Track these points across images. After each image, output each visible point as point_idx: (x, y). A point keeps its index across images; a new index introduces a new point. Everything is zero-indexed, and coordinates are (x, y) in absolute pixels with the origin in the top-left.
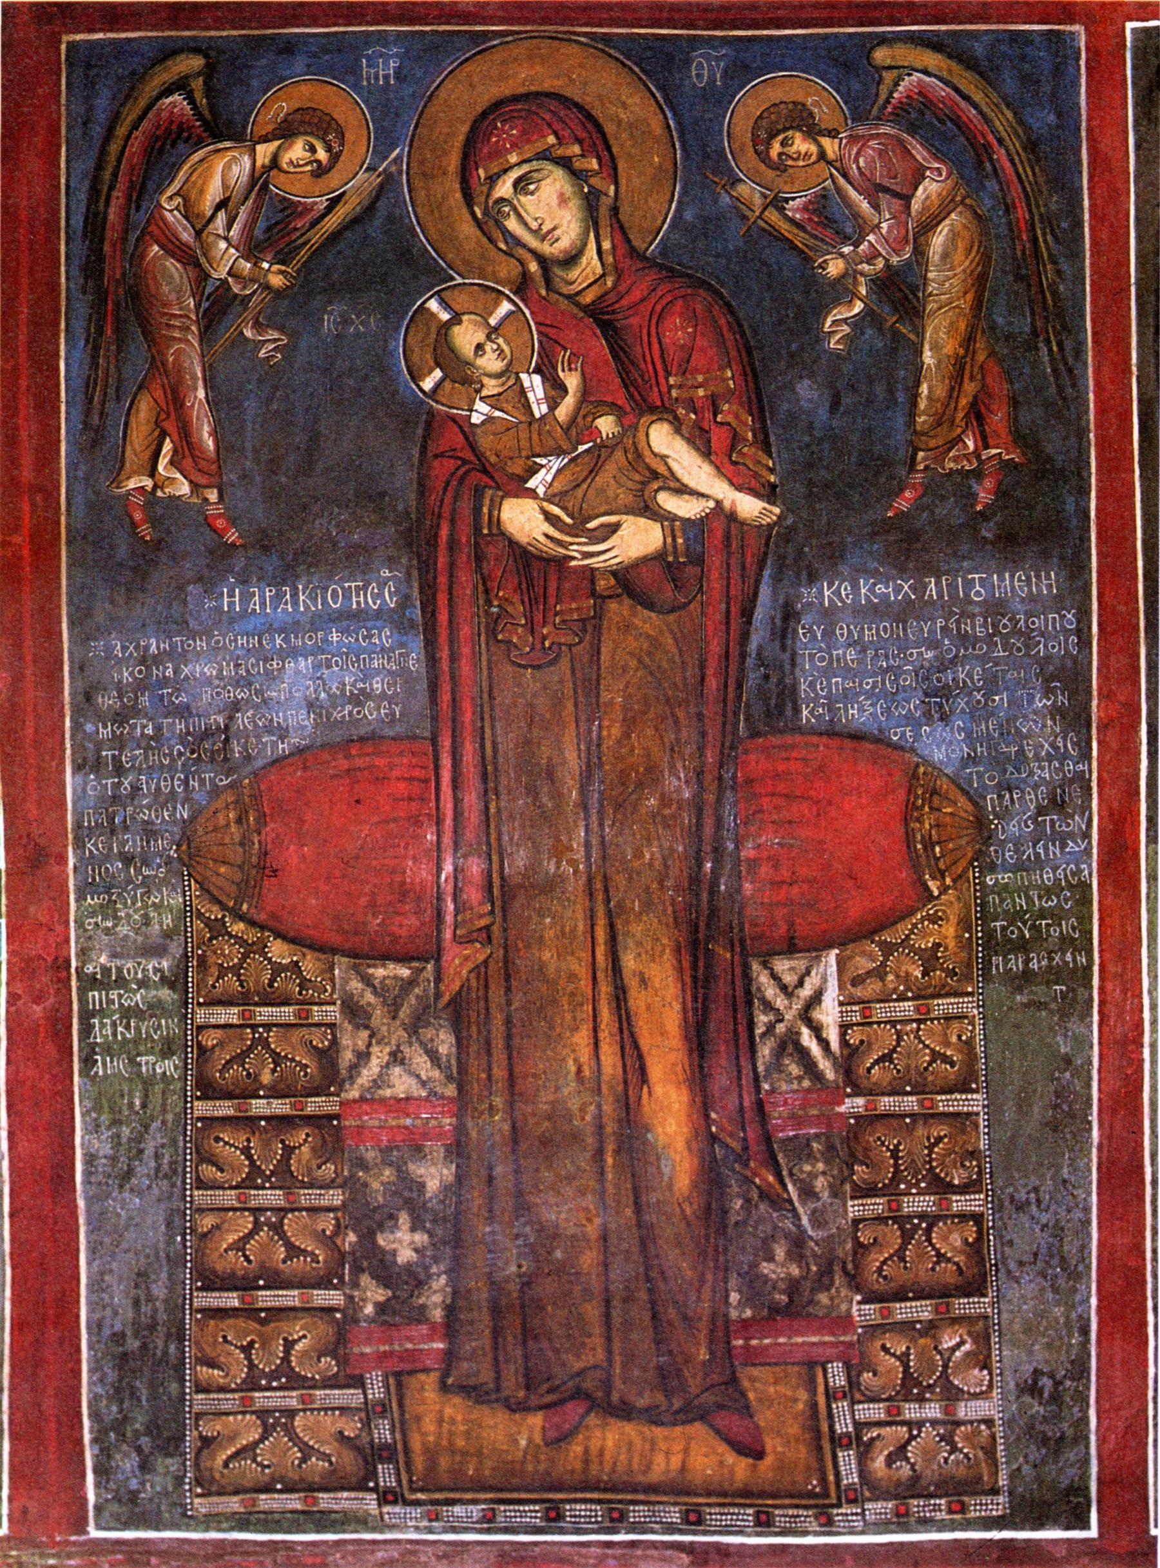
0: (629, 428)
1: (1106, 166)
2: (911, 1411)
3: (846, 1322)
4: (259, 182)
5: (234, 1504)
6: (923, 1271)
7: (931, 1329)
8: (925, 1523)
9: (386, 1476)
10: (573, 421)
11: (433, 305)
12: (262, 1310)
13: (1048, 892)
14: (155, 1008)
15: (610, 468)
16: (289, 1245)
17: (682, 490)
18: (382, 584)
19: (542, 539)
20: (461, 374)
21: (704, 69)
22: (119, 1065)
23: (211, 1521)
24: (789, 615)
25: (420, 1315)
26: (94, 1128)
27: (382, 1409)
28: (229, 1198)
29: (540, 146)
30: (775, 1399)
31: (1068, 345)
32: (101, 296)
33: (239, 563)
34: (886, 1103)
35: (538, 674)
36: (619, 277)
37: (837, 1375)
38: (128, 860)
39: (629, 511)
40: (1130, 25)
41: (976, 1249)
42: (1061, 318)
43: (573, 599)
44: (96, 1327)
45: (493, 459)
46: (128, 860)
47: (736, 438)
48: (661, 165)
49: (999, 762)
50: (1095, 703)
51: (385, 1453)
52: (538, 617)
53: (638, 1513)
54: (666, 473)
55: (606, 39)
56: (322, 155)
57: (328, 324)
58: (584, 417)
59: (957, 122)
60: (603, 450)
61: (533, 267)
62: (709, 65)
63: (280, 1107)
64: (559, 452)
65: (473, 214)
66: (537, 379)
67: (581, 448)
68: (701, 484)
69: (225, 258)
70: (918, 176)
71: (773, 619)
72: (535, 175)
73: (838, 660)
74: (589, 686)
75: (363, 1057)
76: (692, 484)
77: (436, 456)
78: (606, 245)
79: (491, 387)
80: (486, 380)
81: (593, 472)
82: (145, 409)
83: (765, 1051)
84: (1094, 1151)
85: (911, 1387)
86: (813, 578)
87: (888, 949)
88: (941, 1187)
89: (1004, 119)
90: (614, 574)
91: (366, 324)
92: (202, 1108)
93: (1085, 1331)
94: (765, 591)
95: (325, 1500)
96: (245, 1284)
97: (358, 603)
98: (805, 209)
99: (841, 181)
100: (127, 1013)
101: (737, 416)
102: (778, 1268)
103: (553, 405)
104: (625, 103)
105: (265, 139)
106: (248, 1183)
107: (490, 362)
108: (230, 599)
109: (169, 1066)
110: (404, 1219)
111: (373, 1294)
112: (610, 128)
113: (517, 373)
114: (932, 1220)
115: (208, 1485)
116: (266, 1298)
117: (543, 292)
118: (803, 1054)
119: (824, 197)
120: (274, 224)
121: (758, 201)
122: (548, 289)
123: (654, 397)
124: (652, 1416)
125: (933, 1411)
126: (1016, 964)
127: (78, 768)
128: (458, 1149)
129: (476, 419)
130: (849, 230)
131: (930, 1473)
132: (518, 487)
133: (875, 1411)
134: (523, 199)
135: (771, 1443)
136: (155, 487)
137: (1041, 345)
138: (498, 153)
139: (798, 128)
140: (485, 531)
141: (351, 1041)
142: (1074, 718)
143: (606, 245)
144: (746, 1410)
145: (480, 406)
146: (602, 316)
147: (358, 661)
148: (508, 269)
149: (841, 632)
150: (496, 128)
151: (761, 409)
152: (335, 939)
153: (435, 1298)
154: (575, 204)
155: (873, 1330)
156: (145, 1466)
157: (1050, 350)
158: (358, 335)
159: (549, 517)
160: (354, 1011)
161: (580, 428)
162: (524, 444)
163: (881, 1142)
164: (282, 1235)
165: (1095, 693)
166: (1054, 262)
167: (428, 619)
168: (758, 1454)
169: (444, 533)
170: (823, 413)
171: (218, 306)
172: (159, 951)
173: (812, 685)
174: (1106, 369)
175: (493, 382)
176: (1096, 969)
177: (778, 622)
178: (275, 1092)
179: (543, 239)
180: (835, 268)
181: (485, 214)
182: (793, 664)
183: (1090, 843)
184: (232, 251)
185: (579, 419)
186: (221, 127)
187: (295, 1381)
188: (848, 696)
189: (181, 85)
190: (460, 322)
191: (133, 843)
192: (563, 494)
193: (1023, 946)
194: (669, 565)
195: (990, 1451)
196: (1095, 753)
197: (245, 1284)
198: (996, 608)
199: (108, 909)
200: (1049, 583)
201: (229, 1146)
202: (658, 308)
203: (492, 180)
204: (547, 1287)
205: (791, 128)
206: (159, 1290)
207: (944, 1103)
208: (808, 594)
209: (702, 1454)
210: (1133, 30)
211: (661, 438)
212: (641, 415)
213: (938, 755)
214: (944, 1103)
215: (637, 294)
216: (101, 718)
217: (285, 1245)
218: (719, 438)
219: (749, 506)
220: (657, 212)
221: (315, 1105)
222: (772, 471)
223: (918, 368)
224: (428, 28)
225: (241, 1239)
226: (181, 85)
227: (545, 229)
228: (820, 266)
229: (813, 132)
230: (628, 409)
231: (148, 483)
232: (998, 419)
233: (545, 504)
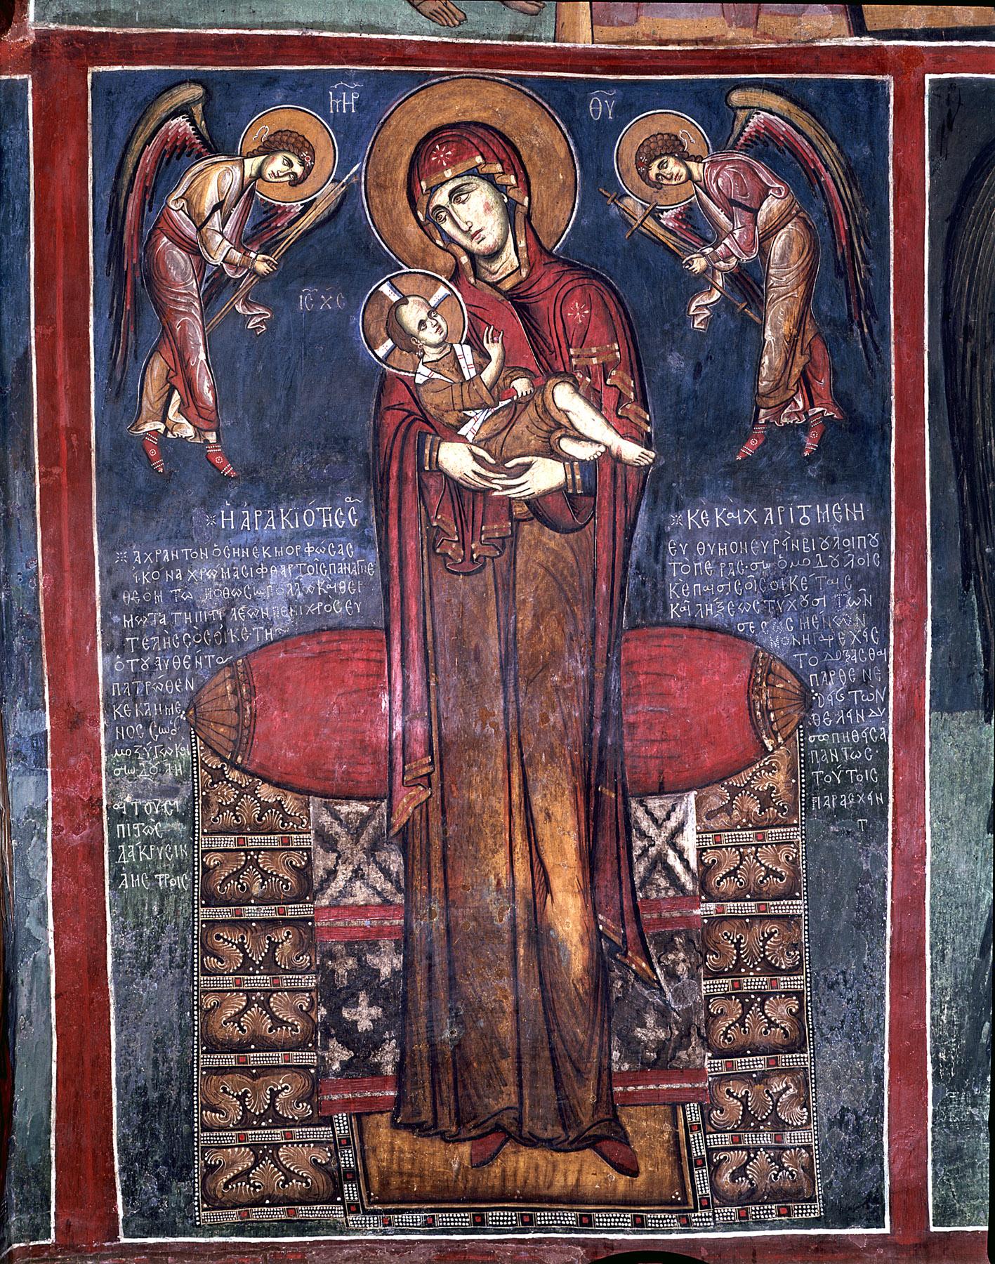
0: (538, 390)
1: (907, 186)
2: (748, 1139)
3: (699, 1073)
4: (248, 189)
5: (233, 1216)
6: (757, 1032)
7: (763, 1077)
8: (761, 1223)
9: (350, 1192)
10: (495, 382)
11: (385, 289)
12: (253, 1068)
13: (856, 748)
14: (170, 837)
15: (524, 420)
16: (273, 1017)
17: (580, 438)
18: (346, 509)
19: (471, 475)
20: (406, 342)
21: (600, 106)
22: (141, 881)
23: (212, 1230)
24: (660, 536)
25: (376, 1070)
26: (121, 929)
27: (348, 1142)
28: (228, 982)
29: (469, 164)
30: (646, 1130)
31: (875, 329)
32: (121, 277)
33: (233, 492)
34: (731, 907)
35: (468, 579)
37: (693, 1113)
38: (147, 722)
39: (537, 454)
40: (928, 77)
41: (797, 1017)
42: (873, 307)
43: (495, 522)
44: (123, 1083)
45: (432, 411)
46: (147, 722)
47: (621, 397)
48: (564, 182)
49: (820, 649)
50: (892, 604)
51: (352, 1175)
52: (468, 536)
53: (542, 1218)
54: (567, 424)
55: (521, 80)
56: (298, 169)
57: (303, 302)
58: (504, 379)
59: (794, 151)
60: (518, 406)
61: (464, 260)
62: (604, 104)
63: (268, 912)
64: (484, 406)
65: (417, 218)
66: (467, 348)
67: (502, 404)
68: (594, 431)
69: (220, 249)
70: (764, 195)
71: (648, 538)
72: (466, 187)
73: (698, 570)
74: (507, 587)
75: (332, 874)
76: (587, 433)
77: (388, 408)
78: (522, 244)
79: (432, 354)
80: (427, 349)
81: (511, 423)
82: (158, 368)
83: (640, 868)
84: (888, 942)
85: (749, 1120)
86: (679, 507)
87: (734, 791)
88: (771, 970)
89: (829, 151)
90: (528, 503)
91: (331, 303)
92: (205, 913)
93: (879, 1079)
94: (642, 517)
95: (303, 1212)
96: (241, 1048)
97: (327, 523)
98: (676, 218)
99: (704, 196)
100: (147, 841)
101: (622, 381)
102: (650, 1033)
103: (480, 368)
104: (542, 135)
105: (252, 155)
106: (243, 970)
107: (430, 335)
108: (227, 519)
109: (180, 881)
110: (363, 998)
111: (340, 1055)
112: (524, 152)
114: (765, 996)
115: (213, 1202)
116: (256, 1059)
117: (472, 280)
118: (669, 870)
119: (691, 209)
120: (260, 221)
121: (639, 213)
122: (476, 277)
123: (559, 366)
124: (551, 1145)
125: (766, 1139)
126: (830, 802)
127: (107, 651)
128: (405, 943)
129: (419, 379)
130: (710, 235)
131: (763, 1185)
132: (452, 433)
133: (724, 1140)
134: (455, 206)
135: (644, 1166)
136: (166, 430)
137: (855, 327)
138: (439, 168)
139: (671, 154)
140: (427, 468)
141: (323, 861)
142: (878, 616)
143: (522, 244)
144: (624, 1140)
145: (421, 369)
146: (519, 300)
147: (327, 568)
148: (444, 261)
149: (701, 549)
150: (435, 149)
151: (641, 376)
152: (306, 783)
153: (387, 1057)
154: (497, 212)
155: (722, 1079)
156: (163, 1189)
157: (862, 332)
158: (327, 311)
159: (477, 458)
160: (327, 841)
161: (499, 388)
162: (457, 401)
163: (727, 936)
164: (269, 1011)
165: (892, 597)
166: (866, 262)
167: (380, 534)
168: (635, 1173)
169: (394, 470)
170: (688, 379)
171: (216, 286)
172: (172, 792)
173: (678, 589)
174: (904, 349)
176: (890, 806)
177: (652, 540)
178: (262, 901)
179: (472, 237)
180: (699, 264)
181: (426, 219)
182: (664, 573)
183: (887, 710)
184: (226, 243)
185: (500, 381)
186: (216, 144)
187: (280, 1122)
188: (704, 597)
189: (183, 110)
190: (407, 303)
191: (152, 710)
192: (487, 440)
193: (835, 789)
194: (569, 496)
195: (808, 1169)
196: (892, 643)
197: (241, 1048)
198: (820, 531)
199: (132, 761)
200: (859, 512)
201: (228, 942)
202: (562, 294)
203: (433, 190)
204: (473, 1048)
205: (666, 154)
206: (173, 1055)
207: (775, 908)
208: (675, 519)
209: (587, 1171)
210: (931, 81)
211: (564, 397)
212: (548, 378)
213: (774, 644)
214: (775, 908)
215: (545, 283)
216: (125, 610)
217: (271, 1018)
218: (609, 398)
219: (631, 451)
220: (560, 217)
221: (294, 911)
222: (648, 423)
223: (761, 343)
224: (382, 68)
225: (236, 1014)
226: (183, 110)
227: (473, 230)
228: (687, 263)
229: (683, 158)
230: (538, 373)
231: (161, 427)
232: (822, 384)
233: (474, 448)
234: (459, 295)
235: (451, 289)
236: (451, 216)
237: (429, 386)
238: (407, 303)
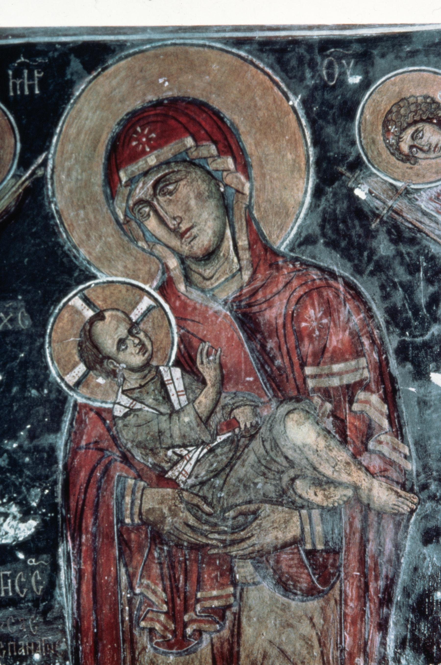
36: (254, 273)
61: (173, 263)
65: (114, 213)
66: (177, 372)
72: (174, 177)
113: (157, 367)
129: (119, 411)
139: (429, 121)
150: (136, 132)
175: (135, 376)
179: (182, 235)
205: (422, 120)
227: (184, 227)
234: (167, 307)
235: (156, 300)
236: (156, 212)
237: (131, 419)
238: (103, 318)
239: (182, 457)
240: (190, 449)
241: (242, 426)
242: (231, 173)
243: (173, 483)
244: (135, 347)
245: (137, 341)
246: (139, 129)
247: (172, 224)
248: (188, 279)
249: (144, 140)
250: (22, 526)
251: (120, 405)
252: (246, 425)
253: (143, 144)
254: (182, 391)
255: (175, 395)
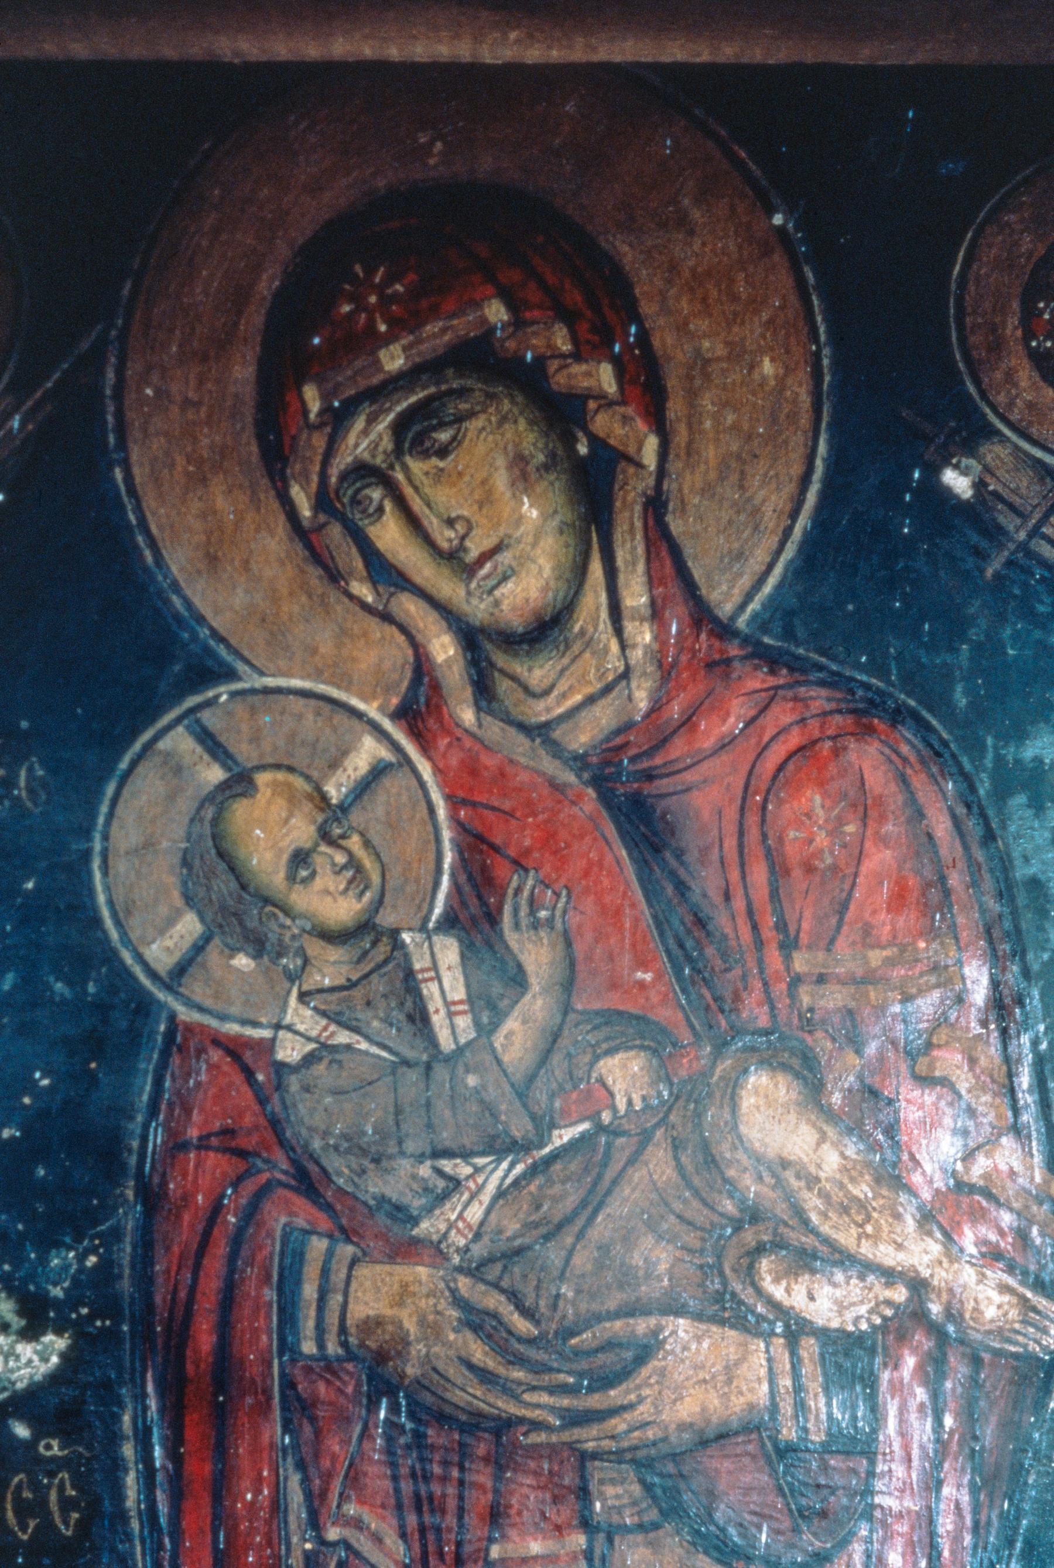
29: (463, 326)
61: (444, 648)
64: (501, 1146)
66: (449, 951)
67: (563, 1136)
113: (395, 933)
134: (417, 466)
138: (364, 342)
175: (335, 954)
179: (469, 571)
227: (474, 549)
239: (455, 1184)
240: (480, 1161)
241: (621, 1104)
242: (611, 404)
243: (435, 1251)
244: (338, 873)
245: (340, 858)
246: (358, 269)
247: (445, 537)
248: (483, 690)
249: (373, 299)
250: (26, 1350)
251: (297, 1031)
252: (630, 1103)
253: (370, 311)
254: (461, 1002)
255: (443, 1012)
